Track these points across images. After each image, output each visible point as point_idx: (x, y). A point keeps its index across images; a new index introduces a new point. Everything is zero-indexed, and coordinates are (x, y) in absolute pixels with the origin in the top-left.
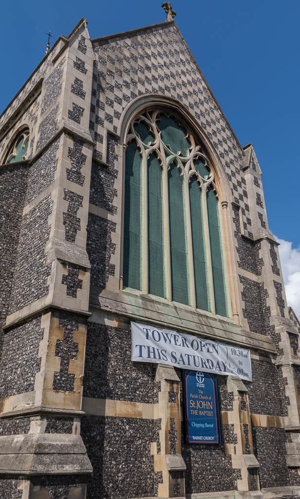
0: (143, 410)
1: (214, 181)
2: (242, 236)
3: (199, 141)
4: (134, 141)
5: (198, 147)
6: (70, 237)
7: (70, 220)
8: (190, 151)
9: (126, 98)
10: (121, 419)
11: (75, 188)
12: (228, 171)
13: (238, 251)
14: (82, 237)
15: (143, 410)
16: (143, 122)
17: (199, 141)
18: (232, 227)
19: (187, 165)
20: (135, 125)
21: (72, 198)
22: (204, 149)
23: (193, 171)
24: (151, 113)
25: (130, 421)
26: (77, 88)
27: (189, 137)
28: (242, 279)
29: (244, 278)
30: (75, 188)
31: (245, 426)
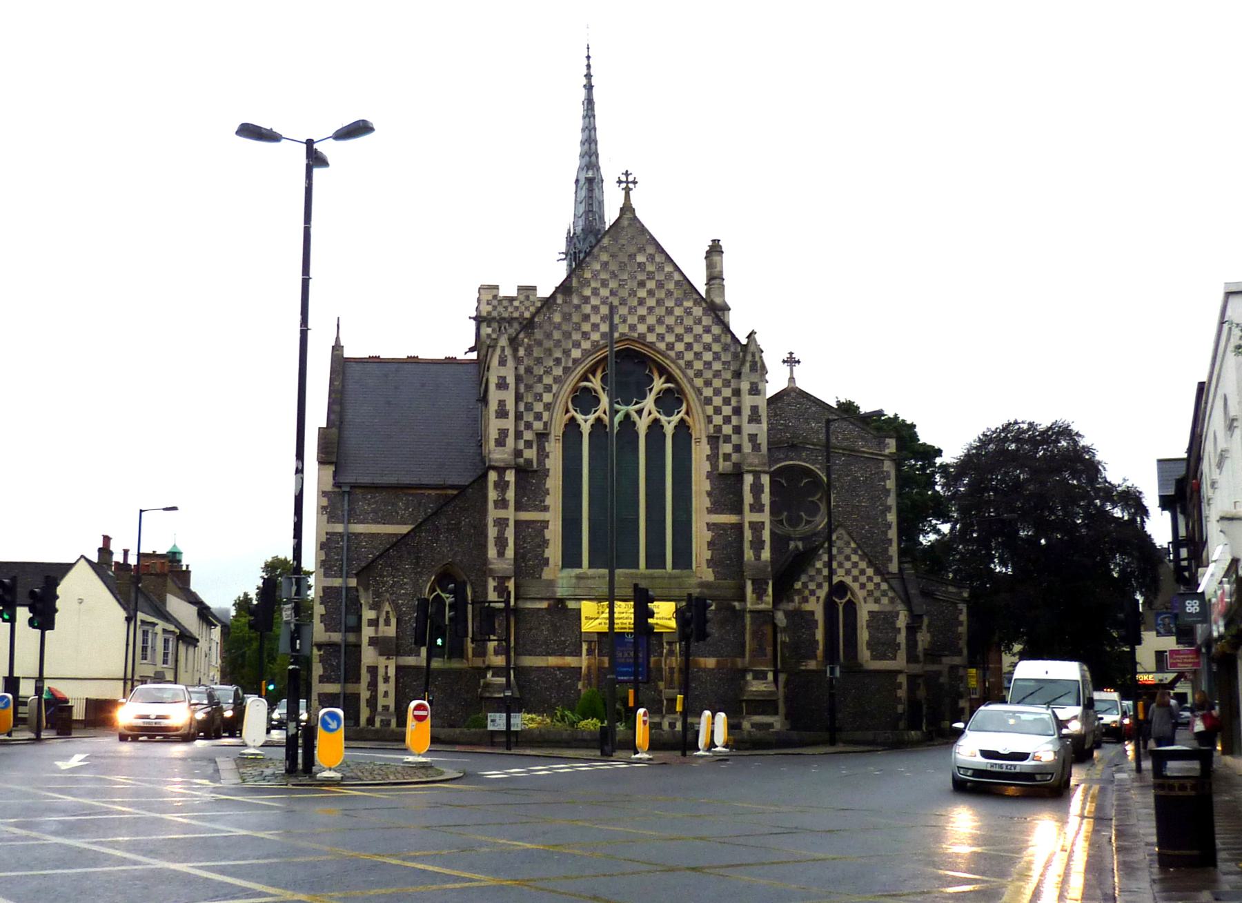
0: (570, 661)
1: (687, 413)
2: (721, 474)
3: (663, 371)
4: (573, 419)
5: (663, 379)
6: (501, 554)
7: (501, 543)
8: (651, 390)
9: (557, 380)
10: (553, 668)
11: (502, 514)
12: (708, 392)
13: (709, 494)
14: (510, 552)
15: (570, 661)
16: (586, 388)
17: (663, 371)
18: (707, 467)
19: (645, 413)
20: (575, 401)
21: (502, 523)
22: (670, 378)
23: (655, 414)
24: (594, 376)
25: (559, 668)
26: (502, 413)
27: (651, 371)
28: (710, 526)
29: (714, 524)
30: (502, 514)
31: (671, 669)
